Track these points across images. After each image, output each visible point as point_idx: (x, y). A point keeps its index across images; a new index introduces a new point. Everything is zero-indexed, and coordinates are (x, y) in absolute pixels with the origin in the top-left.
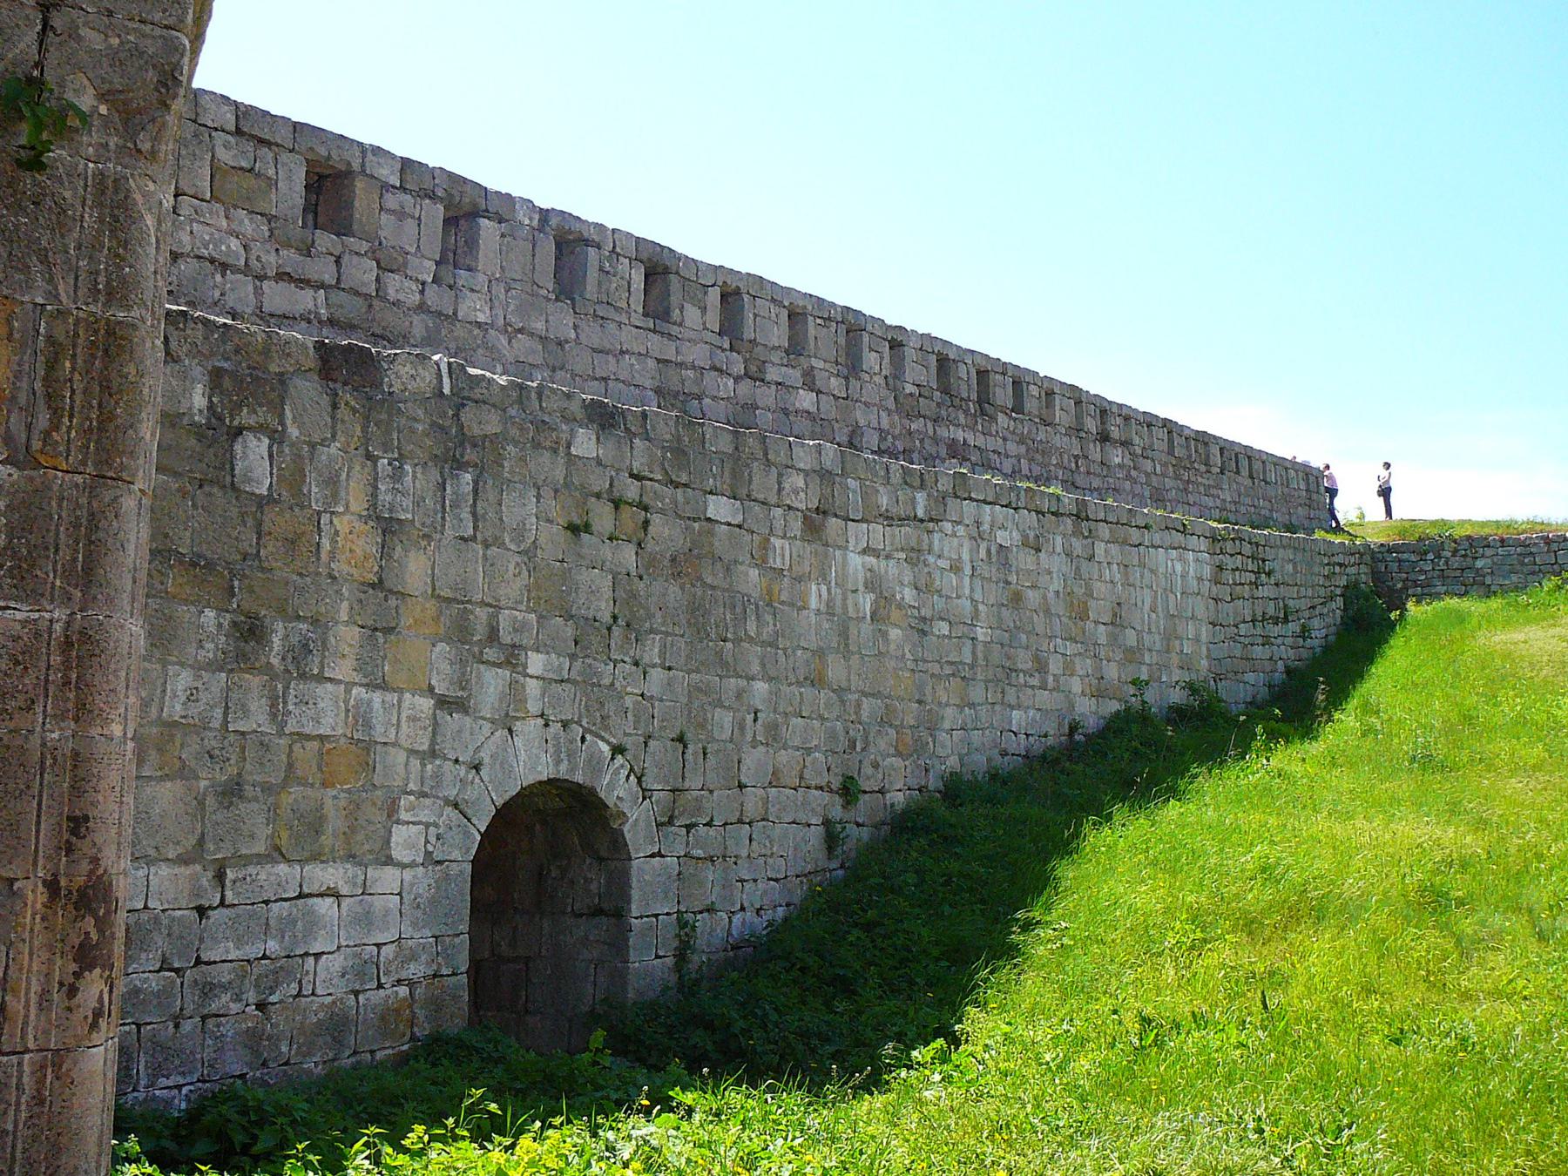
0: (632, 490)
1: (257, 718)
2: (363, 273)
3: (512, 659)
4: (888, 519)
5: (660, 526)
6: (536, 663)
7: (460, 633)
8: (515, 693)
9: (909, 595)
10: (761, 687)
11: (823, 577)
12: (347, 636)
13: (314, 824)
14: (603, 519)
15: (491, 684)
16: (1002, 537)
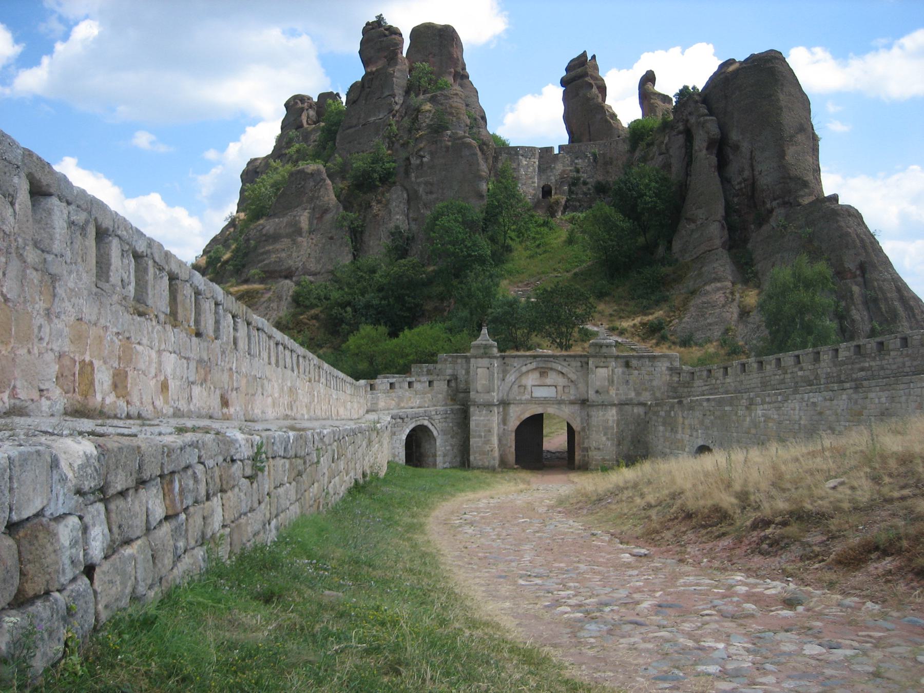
0: (712, 409)
1: (673, 436)
2: (714, 381)
3: (697, 431)
4: (769, 403)
5: (716, 413)
6: (700, 431)
7: (691, 428)
8: (698, 435)
9: (776, 417)
10: (735, 434)
11: (750, 415)
12: (680, 429)
13: (678, 447)
14: (708, 413)
15: (695, 434)
16: (812, 400)
